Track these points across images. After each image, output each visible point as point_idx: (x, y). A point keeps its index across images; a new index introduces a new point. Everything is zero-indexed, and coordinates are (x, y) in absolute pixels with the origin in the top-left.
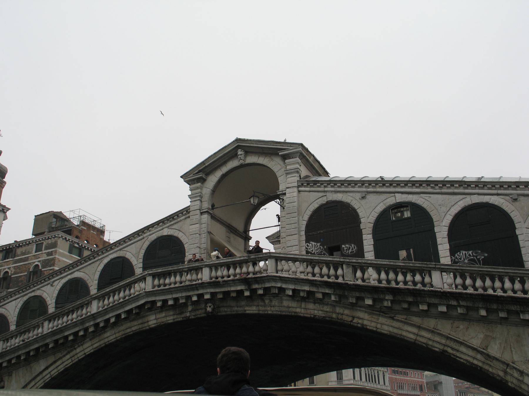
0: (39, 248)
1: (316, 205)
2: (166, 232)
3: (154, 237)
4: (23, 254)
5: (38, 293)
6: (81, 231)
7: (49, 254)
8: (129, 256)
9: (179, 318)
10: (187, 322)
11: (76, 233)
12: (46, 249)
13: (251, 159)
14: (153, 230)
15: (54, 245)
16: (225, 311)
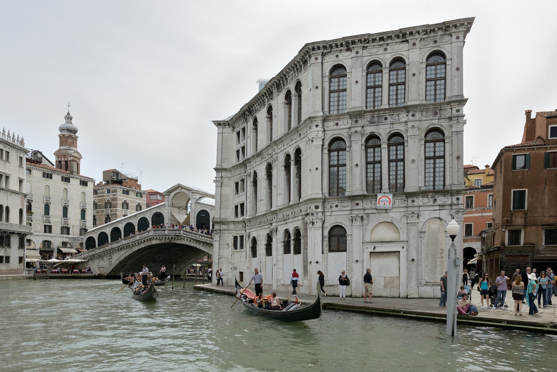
0: (109, 191)
1: (199, 210)
2: (158, 211)
3: (154, 212)
4: (102, 193)
5: (117, 226)
6: (127, 183)
7: (114, 195)
8: (147, 217)
9: (160, 242)
10: (162, 243)
11: (124, 184)
12: (112, 192)
13: (183, 190)
14: (154, 209)
15: (116, 191)
16: (172, 242)
